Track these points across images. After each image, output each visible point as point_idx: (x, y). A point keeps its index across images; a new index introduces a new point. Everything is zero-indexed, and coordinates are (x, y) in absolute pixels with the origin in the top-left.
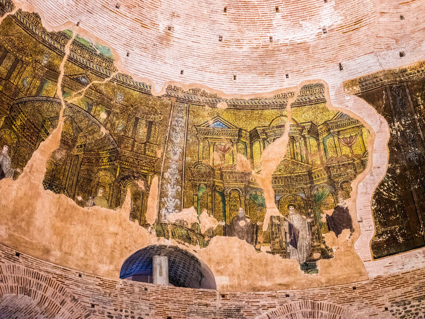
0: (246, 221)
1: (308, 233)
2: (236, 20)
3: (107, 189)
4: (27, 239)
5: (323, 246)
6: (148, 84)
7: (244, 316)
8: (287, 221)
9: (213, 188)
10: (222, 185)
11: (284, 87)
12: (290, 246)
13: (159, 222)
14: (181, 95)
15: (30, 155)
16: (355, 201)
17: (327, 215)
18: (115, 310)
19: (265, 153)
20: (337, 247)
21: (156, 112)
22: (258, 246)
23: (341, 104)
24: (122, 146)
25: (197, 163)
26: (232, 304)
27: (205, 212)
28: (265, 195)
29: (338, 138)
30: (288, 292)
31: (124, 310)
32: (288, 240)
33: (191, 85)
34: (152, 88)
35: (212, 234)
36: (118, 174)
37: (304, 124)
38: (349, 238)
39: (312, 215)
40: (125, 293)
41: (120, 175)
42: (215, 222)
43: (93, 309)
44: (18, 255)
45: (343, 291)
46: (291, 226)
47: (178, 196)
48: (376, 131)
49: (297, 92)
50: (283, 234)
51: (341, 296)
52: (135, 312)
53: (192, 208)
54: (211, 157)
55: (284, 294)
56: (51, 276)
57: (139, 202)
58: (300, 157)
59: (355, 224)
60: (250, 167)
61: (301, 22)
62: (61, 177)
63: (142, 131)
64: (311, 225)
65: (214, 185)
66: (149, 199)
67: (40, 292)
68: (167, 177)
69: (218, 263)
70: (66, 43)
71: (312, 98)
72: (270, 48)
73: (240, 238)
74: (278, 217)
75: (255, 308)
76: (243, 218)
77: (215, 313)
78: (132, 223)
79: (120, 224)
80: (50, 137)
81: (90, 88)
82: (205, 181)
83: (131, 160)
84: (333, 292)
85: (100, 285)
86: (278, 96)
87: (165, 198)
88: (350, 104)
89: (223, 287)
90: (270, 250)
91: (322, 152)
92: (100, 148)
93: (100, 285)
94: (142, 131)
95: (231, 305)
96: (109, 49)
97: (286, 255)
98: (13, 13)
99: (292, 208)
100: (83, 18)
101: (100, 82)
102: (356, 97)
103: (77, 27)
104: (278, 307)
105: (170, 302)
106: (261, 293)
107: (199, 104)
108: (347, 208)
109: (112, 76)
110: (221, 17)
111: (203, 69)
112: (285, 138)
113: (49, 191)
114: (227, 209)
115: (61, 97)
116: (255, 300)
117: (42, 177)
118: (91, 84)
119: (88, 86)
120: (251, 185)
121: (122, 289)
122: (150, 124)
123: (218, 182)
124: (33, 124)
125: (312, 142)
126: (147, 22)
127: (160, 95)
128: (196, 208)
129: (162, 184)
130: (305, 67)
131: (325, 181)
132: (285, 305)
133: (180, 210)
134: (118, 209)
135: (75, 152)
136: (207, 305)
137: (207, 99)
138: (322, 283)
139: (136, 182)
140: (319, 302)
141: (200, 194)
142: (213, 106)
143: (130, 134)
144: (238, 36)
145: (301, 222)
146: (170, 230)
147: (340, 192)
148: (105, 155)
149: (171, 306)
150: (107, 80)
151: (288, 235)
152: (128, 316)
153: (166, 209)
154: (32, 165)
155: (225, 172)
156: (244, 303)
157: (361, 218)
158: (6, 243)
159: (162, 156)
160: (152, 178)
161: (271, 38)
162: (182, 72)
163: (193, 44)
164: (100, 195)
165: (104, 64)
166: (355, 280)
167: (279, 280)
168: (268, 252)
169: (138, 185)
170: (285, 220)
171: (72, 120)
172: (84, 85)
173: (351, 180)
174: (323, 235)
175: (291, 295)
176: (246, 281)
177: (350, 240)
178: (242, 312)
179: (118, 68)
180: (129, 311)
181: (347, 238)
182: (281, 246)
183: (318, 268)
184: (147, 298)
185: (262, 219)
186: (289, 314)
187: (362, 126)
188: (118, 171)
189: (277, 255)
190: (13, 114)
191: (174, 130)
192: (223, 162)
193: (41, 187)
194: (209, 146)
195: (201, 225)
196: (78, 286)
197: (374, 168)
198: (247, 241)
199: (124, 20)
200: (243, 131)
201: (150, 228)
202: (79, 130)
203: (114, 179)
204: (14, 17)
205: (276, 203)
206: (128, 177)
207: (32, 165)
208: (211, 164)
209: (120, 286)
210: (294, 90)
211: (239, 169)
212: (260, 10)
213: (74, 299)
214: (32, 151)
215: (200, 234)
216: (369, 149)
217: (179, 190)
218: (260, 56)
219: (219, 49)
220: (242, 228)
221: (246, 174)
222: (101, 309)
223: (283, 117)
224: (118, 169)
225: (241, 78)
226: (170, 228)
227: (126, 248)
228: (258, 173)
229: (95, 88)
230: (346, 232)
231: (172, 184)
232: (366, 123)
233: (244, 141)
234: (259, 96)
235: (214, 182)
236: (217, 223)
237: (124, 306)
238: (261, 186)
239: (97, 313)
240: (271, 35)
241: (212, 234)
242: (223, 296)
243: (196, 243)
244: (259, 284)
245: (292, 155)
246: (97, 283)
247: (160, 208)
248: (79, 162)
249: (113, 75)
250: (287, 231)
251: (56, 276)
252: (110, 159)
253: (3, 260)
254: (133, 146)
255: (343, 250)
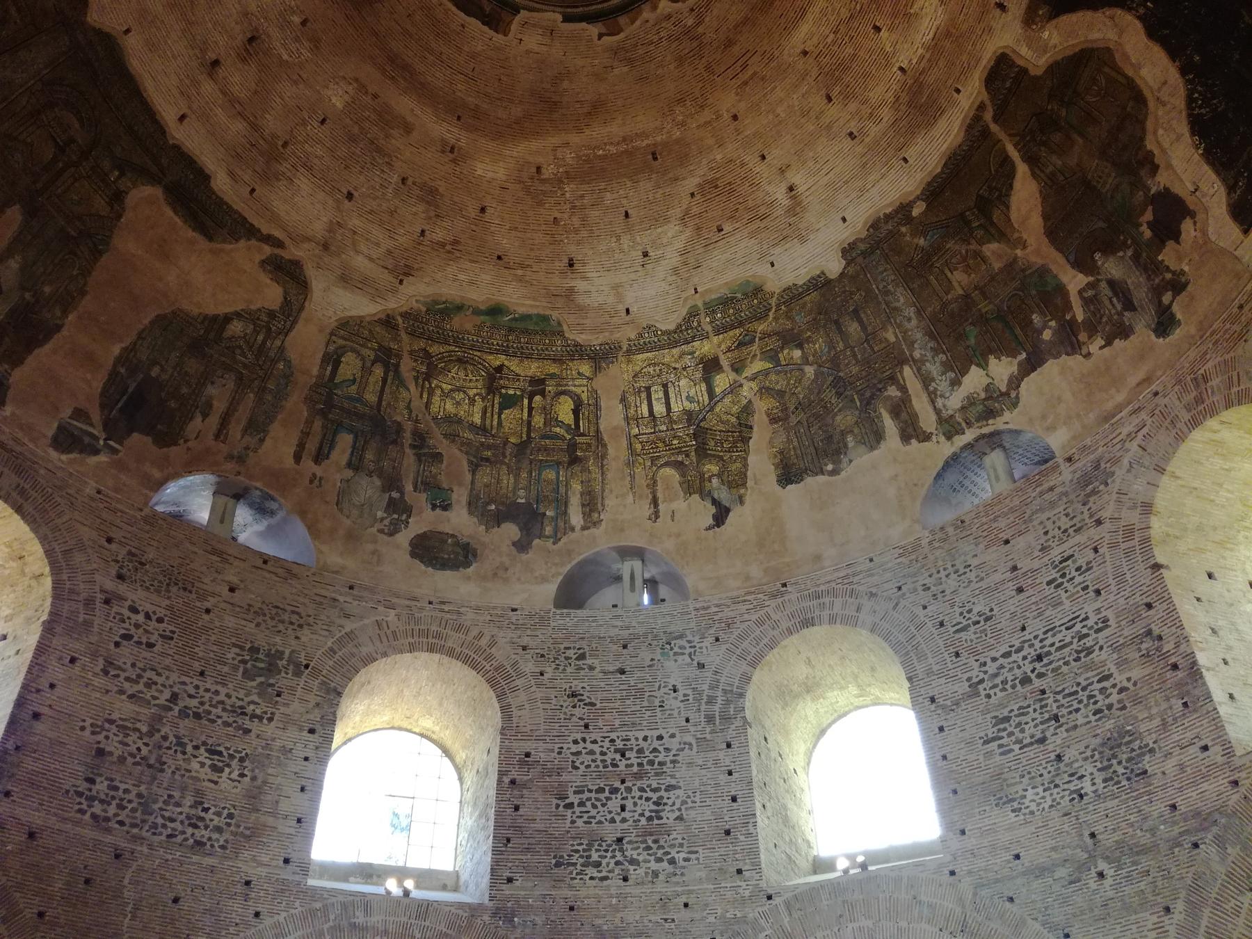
0: (1050, 328)
1: (1138, 273)
2: (847, 96)
3: (856, 431)
4: (787, 560)
5: (1168, 276)
6: (818, 273)
7: (1108, 470)
8: (1101, 280)
9: (982, 320)
10: (991, 306)
11: (967, 108)
12: (1126, 314)
13: (941, 420)
14: (862, 247)
15: (745, 466)
16: (1169, 167)
17: (1148, 223)
18: (930, 576)
19: (1014, 215)
20: (1186, 261)
21: (851, 293)
22: (1084, 351)
23: (1045, 52)
24: (842, 367)
25: (944, 305)
26: (1085, 463)
27: (992, 361)
28: (1054, 268)
29: (1082, 99)
30: (1154, 387)
31: (941, 569)
32: (1119, 307)
33: (866, 223)
34: (826, 271)
35: (1015, 382)
36: (858, 404)
37: (1029, 127)
38: (1195, 230)
39: (1129, 242)
40: (937, 545)
41: (861, 401)
42: (1011, 362)
43: (900, 593)
44: (784, 585)
45: (1228, 326)
46: (1112, 283)
47: (947, 367)
48: (1116, 38)
49: (985, 96)
50: (1107, 302)
51: (1228, 336)
52: (957, 562)
53: (973, 368)
54: (955, 284)
55: (1149, 396)
56: (833, 584)
57: (904, 416)
58: (1059, 174)
59: (1190, 201)
60: (1009, 251)
61: (912, 11)
62: (795, 461)
63: (853, 328)
64: (1136, 258)
65: (982, 316)
66: (914, 402)
67: (826, 613)
68: (919, 356)
69: (1044, 417)
70: (699, 323)
71: (1008, 85)
72: (910, 82)
73: (1056, 358)
74: (1090, 286)
75: (1119, 446)
76: (1045, 327)
77: (1066, 494)
78: (908, 448)
79: (895, 460)
80: (755, 429)
81: (760, 339)
82: (967, 320)
83: (864, 373)
84: (1215, 337)
85: (901, 555)
86: (970, 127)
87: (933, 384)
88: (1055, 39)
89: (1063, 447)
90: (1103, 343)
91: (1080, 141)
92: (818, 393)
93: (901, 555)
94: (853, 328)
95: (1084, 465)
96: (748, 281)
97: (1124, 332)
98: (625, 349)
99: (1097, 256)
100: (696, 280)
101: (766, 324)
102: (1054, 22)
103: (698, 295)
104: (1149, 422)
105: (1000, 519)
106: (1118, 417)
107: (892, 234)
108: (1165, 188)
109: (774, 304)
110: (833, 111)
111: (862, 191)
112: (1022, 169)
113: (789, 487)
114: (1018, 331)
115: (738, 378)
116: (1114, 435)
117: (773, 478)
118: (758, 335)
119: (757, 339)
120: (1027, 273)
121: (930, 543)
122: (856, 312)
123: (984, 307)
124: (729, 431)
125: (1057, 137)
126: (763, 210)
127: (841, 271)
128: (978, 365)
129: (919, 370)
130: (964, 57)
131: (1113, 174)
132: (1157, 412)
133: (959, 383)
134: (883, 445)
135: (793, 420)
136: (1051, 489)
137: (896, 220)
138: (1193, 337)
139: (886, 394)
140: (1202, 371)
141: (972, 341)
142: (909, 219)
143: (841, 346)
144: (866, 110)
145: (1121, 266)
146: (960, 420)
147: (1142, 173)
148: (830, 396)
149: (1002, 523)
150: (771, 314)
151: (1114, 300)
152: (949, 574)
153: (942, 396)
154: (755, 475)
155: (985, 285)
156: (1101, 449)
157: (1194, 183)
158: (764, 581)
159: (896, 337)
160: (901, 372)
161: (901, 69)
162: (844, 220)
163: (829, 176)
164: (851, 445)
165: (755, 301)
166: (1235, 294)
167: (1132, 381)
168: (1101, 348)
169: (889, 396)
170: (1098, 281)
171: (764, 391)
172: (752, 341)
173: (1142, 139)
174: (1160, 258)
175: (1160, 389)
176: (1091, 415)
177: (1199, 234)
178: (1103, 466)
179: (773, 290)
180: (949, 566)
181: (1193, 233)
182: (1114, 325)
183: (1179, 316)
184: (969, 533)
185: (1068, 306)
186: (1166, 423)
187: (1093, 50)
188: (857, 400)
189: (1117, 343)
190: (700, 440)
191: (887, 293)
192: (973, 275)
193: (778, 488)
194: (943, 272)
195: (995, 382)
196: (872, 575)
197: (1159, 90)
198: (1068, 354)
199: (738, 236)
200: (967, 213)
201: (934, 437)
202: (780, 394)
203: (857, 413)
204: (628, 351)
205: (1073, 268)
206: (872, 397)
207: (755, 475)
208: (961, 292)
209: (928, 540)
210: (980, 100)
211: (997, 265)
212: (861, 53)
213: (872, 595)
214: (746, 459)
215: (1002, 394)
216: (1130, 73)
217: (944, 358)
218: (909, 104)
219: (859, 149)
220: (1050, 341)
221: (1011, 266)
222: (913, 585)
223: (997, 147)
224: (855, 397)
225: (911, 153)
226: (959, 418)
227: (915, 485)
228: (1025, 247)
229: (766, 335)
230: (1187, 226)
231: (930, 358)
232: (1095, 41)
233: (977, 224)
234: (948, 153)
235: (980, 310)
236: (1016, 362)
237: (940, 563)
238: (1040, 262)
239: (908, 595)
240: (897, 65)
241: (1015, 382)
242: (1069, 460)
243: (1002, 410)
244: (1110, 405)
245: (1049, 182)
246: (897, 556)
247: (933, 402)
248: (806, 427)
249: (773, 302)
250: (1110, 294)
251: (840, 581)
252: (839, 394)
253: (767, 603)
254: (855, 356)
255: (1197, 258)
